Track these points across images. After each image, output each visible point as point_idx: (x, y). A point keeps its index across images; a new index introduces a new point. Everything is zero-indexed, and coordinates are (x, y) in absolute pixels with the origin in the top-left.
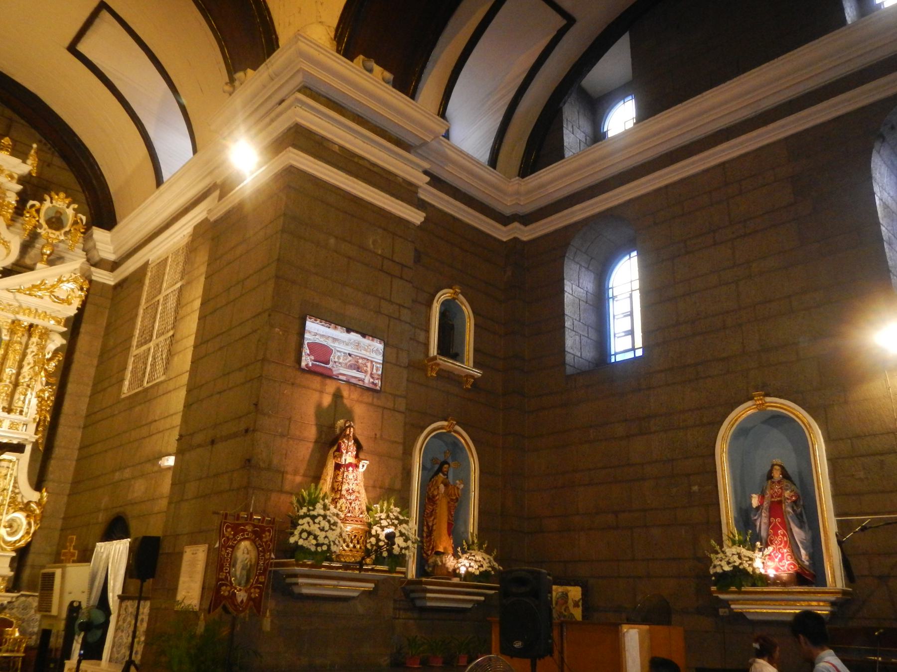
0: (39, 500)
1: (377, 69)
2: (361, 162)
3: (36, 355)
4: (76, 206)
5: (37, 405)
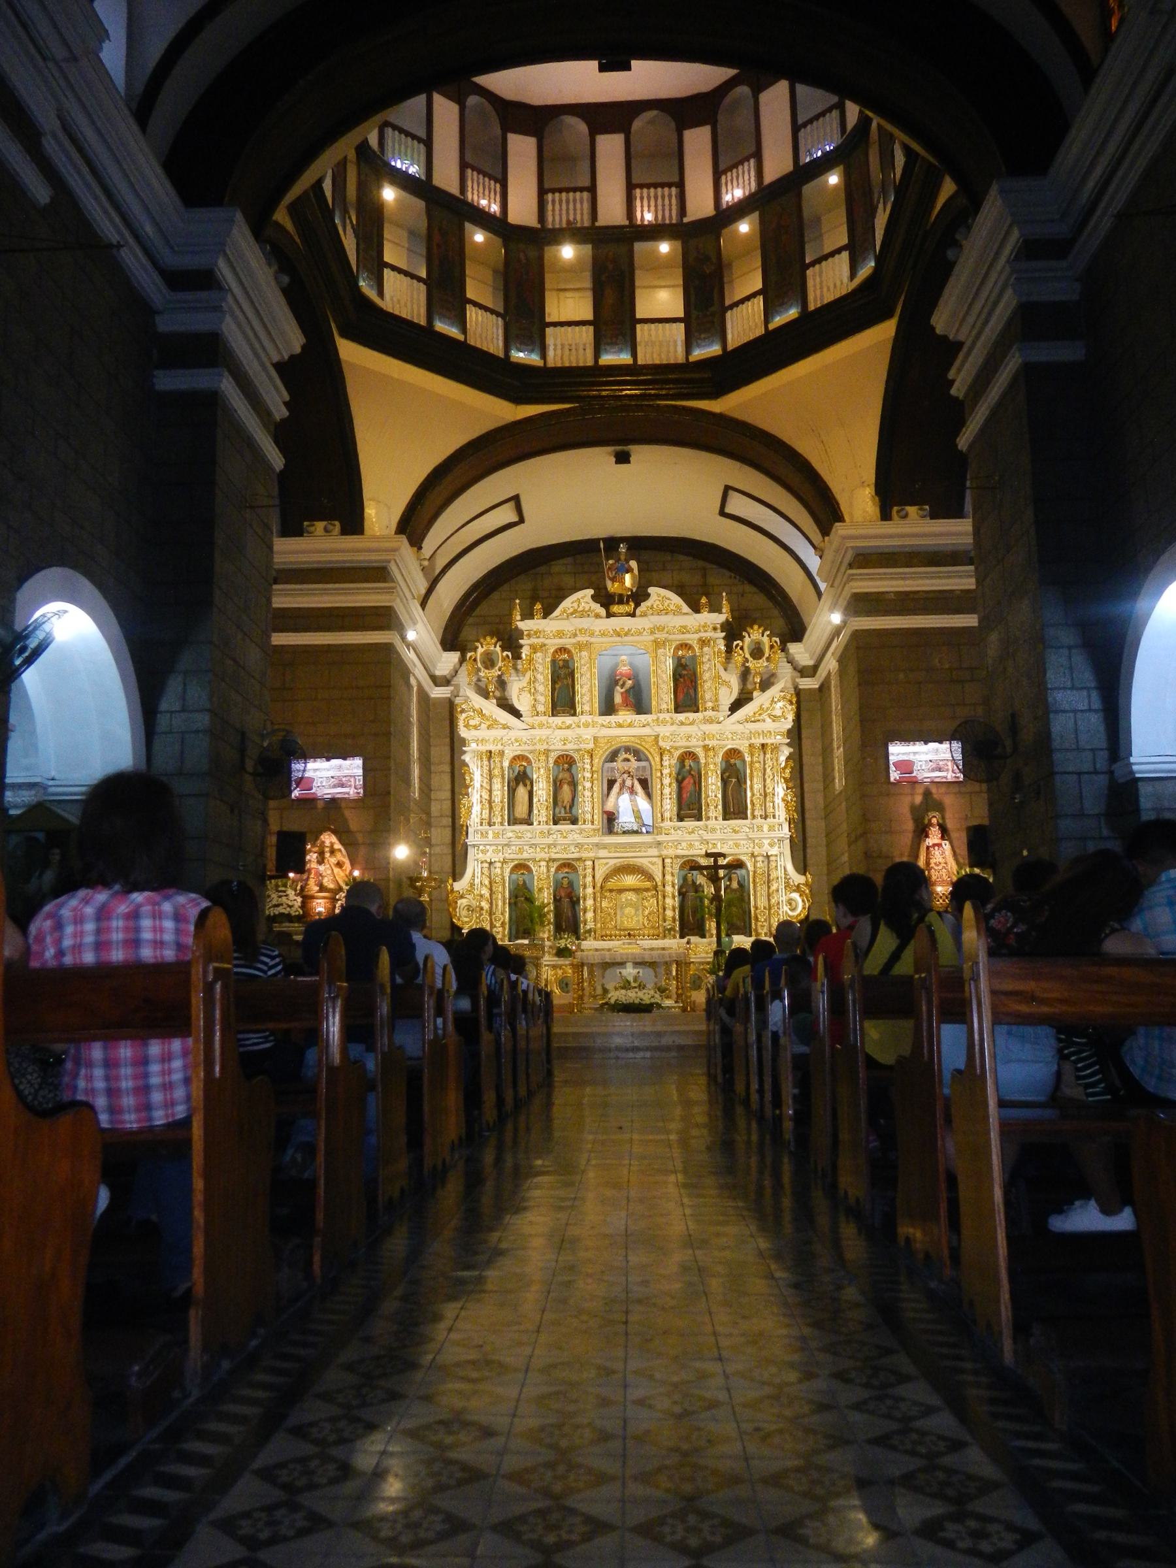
1: (912, 510)
2: (916, 596)
4: (768, 633)
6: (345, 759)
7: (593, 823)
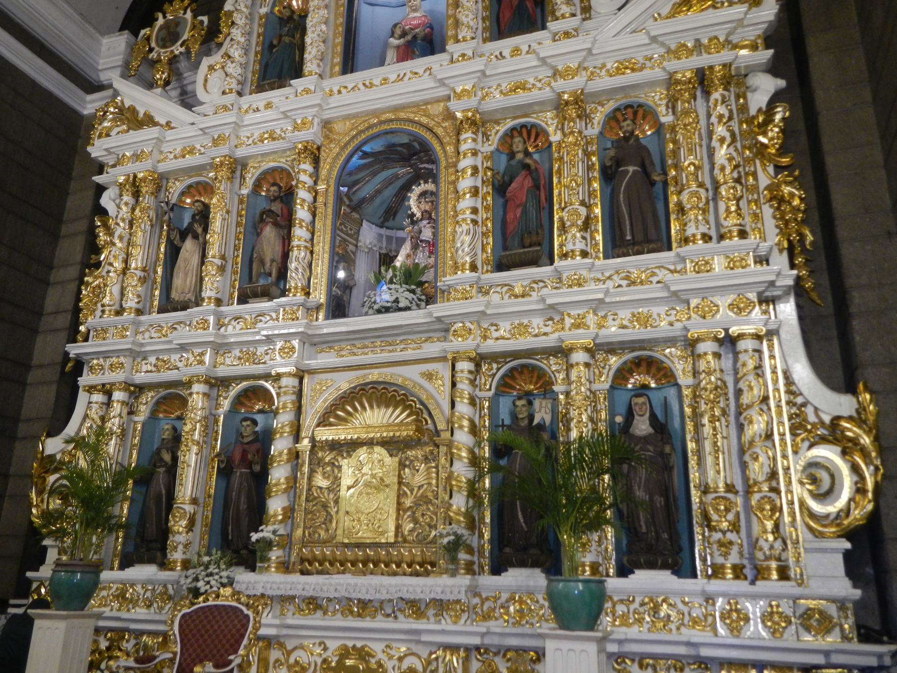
0: (857, 411)
3: (730, 118)
5: (774, 217)
7: (308, 294)
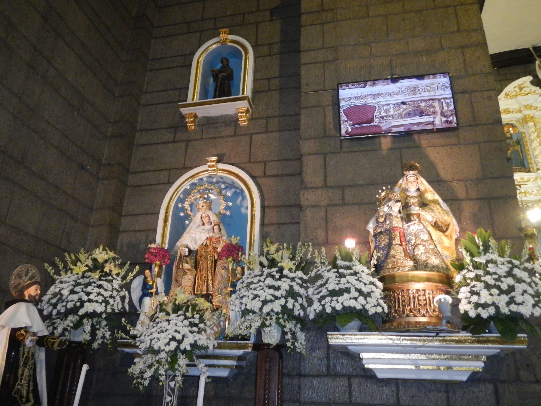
6: (420, 77)
